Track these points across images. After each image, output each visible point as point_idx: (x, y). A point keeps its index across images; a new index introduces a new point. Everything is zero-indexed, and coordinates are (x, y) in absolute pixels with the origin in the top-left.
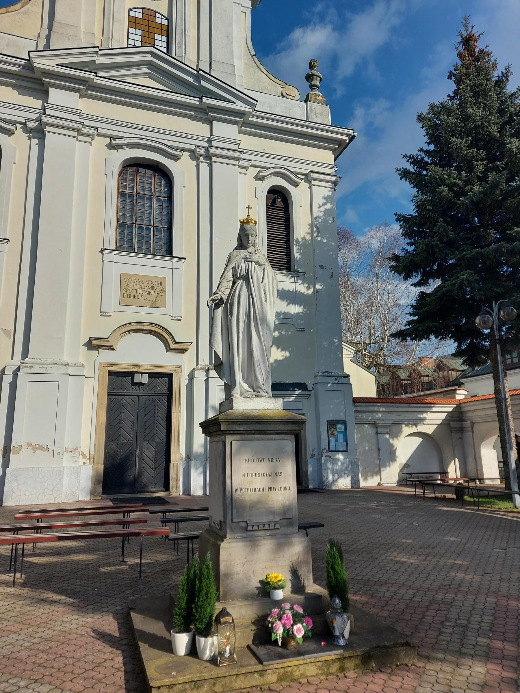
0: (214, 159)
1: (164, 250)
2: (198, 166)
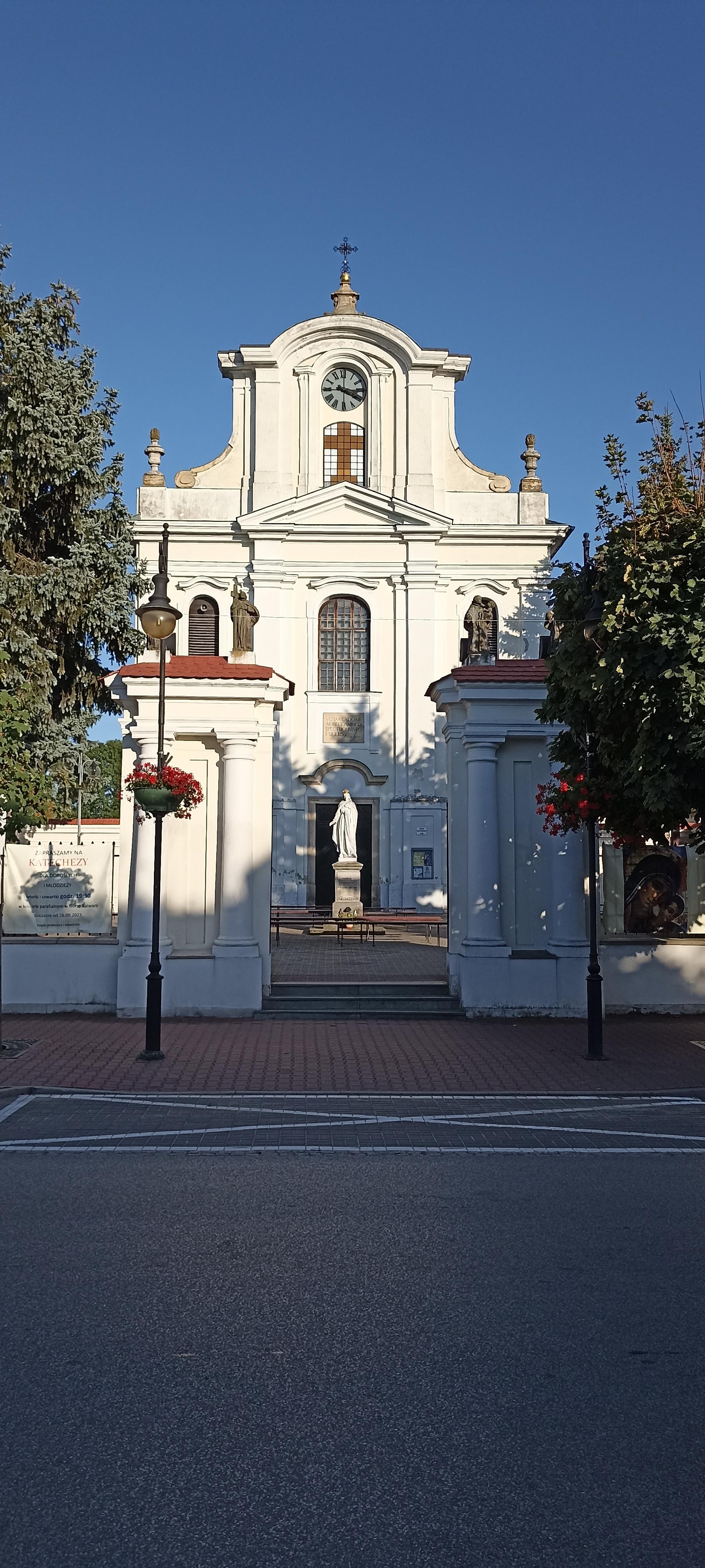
0: (410, 586)
1: (363, 682)
2: (394, 592)
